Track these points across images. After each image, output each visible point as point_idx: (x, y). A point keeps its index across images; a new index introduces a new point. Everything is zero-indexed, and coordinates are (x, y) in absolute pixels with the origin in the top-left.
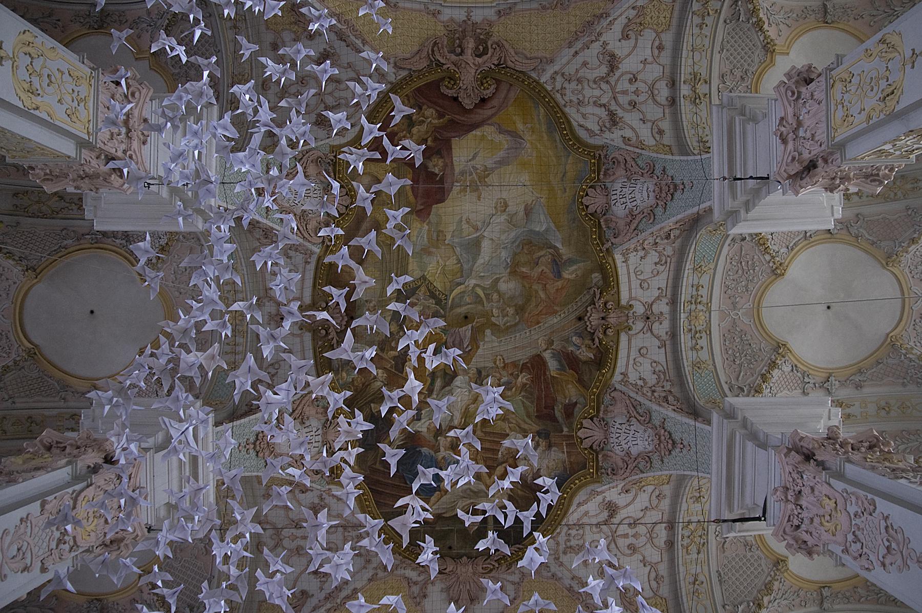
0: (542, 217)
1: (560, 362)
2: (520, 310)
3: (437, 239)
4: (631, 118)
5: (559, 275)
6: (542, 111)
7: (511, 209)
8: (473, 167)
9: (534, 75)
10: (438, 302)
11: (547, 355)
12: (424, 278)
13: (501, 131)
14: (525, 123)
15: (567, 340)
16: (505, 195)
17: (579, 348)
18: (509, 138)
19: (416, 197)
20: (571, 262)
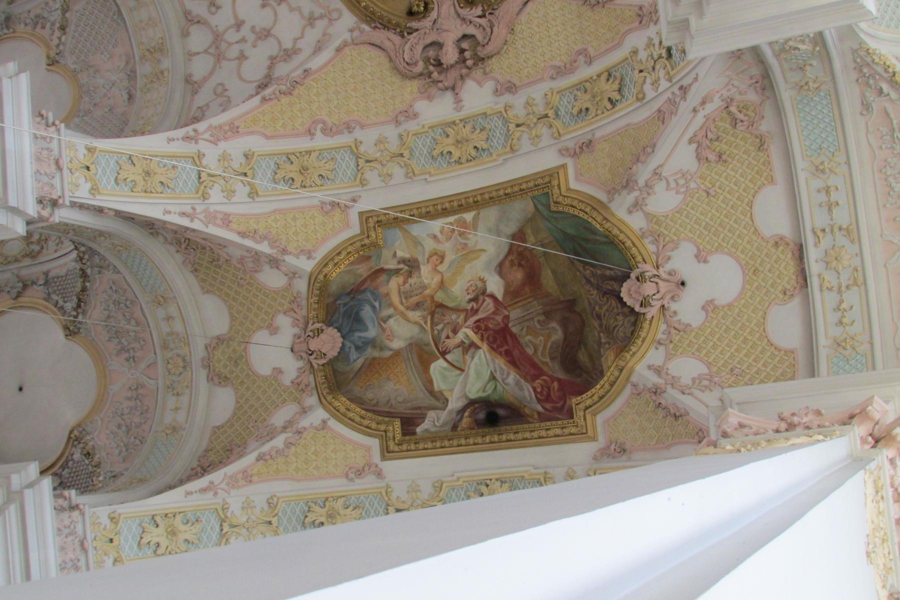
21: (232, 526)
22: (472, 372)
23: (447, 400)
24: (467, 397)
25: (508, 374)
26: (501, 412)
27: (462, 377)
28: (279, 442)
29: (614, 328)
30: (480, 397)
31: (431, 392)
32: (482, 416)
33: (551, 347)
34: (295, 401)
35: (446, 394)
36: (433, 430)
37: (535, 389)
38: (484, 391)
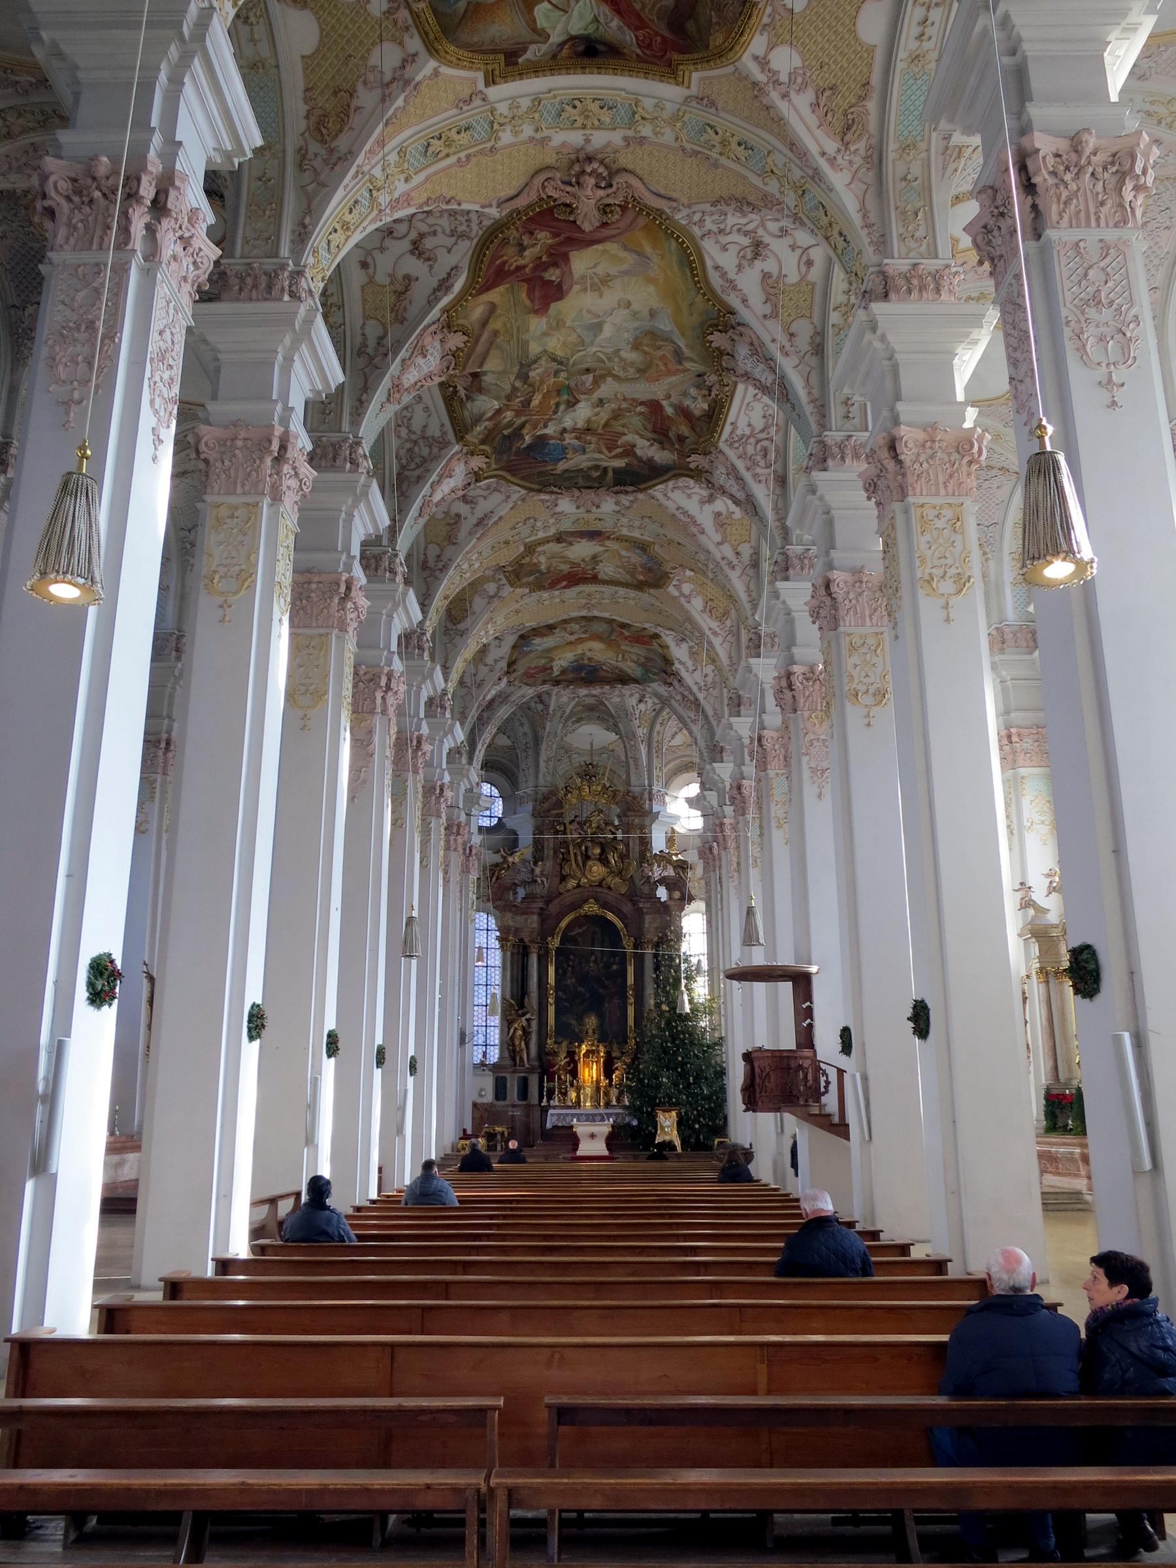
0: (667, 322)
1: (676, 410)
2: (639, 371)
3: (559, 324)
4: (778, 246)
5: (680, 363)
6: (674, 244)
7: (635, 306)
8: (594, 273)
9: (668, 211)
10: (561, 363)
11: (664, 403)
12: (546, 351)
13: (626, 248)
14: (654, 248)
15: (685, 394)
16: (628, 297)
17: (695, 398)
18: (635, 256)
19: (532, 301)
20: (692, 360)
21: (378, 190)
22: (575, 14)
23: (549, 36)
24: (568, 34)
25: (612, 20)
26: (600, 48)
27: (564, 18)
28: (400, 102)
29: (724, 7)
30: (582, 35)
31: (534, 30)
32: (581, 48)
33: (660, 9)
34: (394, 41)
35: (547, 30)
36: (534, 59)
37: (637, 37)
38: (585, 30)
